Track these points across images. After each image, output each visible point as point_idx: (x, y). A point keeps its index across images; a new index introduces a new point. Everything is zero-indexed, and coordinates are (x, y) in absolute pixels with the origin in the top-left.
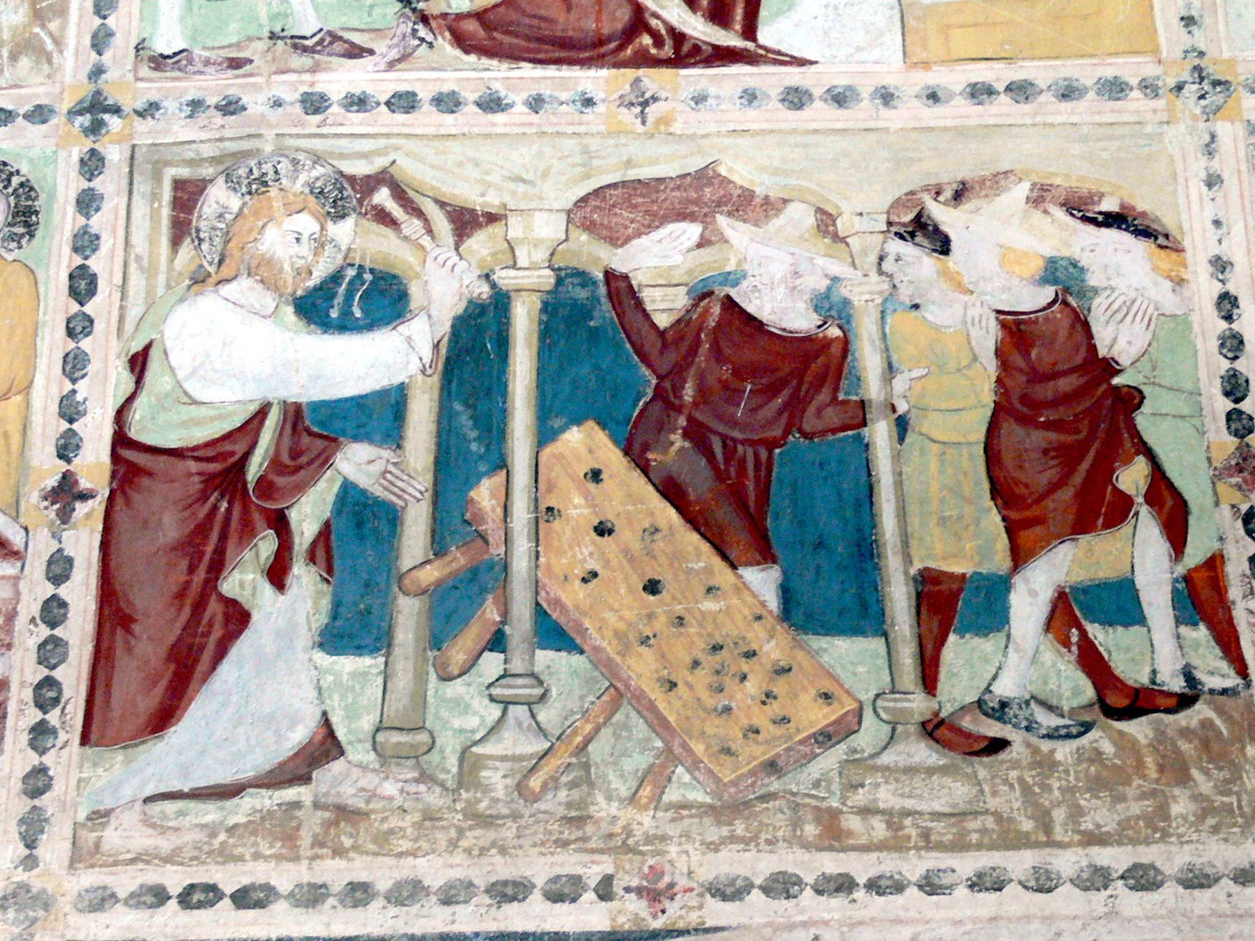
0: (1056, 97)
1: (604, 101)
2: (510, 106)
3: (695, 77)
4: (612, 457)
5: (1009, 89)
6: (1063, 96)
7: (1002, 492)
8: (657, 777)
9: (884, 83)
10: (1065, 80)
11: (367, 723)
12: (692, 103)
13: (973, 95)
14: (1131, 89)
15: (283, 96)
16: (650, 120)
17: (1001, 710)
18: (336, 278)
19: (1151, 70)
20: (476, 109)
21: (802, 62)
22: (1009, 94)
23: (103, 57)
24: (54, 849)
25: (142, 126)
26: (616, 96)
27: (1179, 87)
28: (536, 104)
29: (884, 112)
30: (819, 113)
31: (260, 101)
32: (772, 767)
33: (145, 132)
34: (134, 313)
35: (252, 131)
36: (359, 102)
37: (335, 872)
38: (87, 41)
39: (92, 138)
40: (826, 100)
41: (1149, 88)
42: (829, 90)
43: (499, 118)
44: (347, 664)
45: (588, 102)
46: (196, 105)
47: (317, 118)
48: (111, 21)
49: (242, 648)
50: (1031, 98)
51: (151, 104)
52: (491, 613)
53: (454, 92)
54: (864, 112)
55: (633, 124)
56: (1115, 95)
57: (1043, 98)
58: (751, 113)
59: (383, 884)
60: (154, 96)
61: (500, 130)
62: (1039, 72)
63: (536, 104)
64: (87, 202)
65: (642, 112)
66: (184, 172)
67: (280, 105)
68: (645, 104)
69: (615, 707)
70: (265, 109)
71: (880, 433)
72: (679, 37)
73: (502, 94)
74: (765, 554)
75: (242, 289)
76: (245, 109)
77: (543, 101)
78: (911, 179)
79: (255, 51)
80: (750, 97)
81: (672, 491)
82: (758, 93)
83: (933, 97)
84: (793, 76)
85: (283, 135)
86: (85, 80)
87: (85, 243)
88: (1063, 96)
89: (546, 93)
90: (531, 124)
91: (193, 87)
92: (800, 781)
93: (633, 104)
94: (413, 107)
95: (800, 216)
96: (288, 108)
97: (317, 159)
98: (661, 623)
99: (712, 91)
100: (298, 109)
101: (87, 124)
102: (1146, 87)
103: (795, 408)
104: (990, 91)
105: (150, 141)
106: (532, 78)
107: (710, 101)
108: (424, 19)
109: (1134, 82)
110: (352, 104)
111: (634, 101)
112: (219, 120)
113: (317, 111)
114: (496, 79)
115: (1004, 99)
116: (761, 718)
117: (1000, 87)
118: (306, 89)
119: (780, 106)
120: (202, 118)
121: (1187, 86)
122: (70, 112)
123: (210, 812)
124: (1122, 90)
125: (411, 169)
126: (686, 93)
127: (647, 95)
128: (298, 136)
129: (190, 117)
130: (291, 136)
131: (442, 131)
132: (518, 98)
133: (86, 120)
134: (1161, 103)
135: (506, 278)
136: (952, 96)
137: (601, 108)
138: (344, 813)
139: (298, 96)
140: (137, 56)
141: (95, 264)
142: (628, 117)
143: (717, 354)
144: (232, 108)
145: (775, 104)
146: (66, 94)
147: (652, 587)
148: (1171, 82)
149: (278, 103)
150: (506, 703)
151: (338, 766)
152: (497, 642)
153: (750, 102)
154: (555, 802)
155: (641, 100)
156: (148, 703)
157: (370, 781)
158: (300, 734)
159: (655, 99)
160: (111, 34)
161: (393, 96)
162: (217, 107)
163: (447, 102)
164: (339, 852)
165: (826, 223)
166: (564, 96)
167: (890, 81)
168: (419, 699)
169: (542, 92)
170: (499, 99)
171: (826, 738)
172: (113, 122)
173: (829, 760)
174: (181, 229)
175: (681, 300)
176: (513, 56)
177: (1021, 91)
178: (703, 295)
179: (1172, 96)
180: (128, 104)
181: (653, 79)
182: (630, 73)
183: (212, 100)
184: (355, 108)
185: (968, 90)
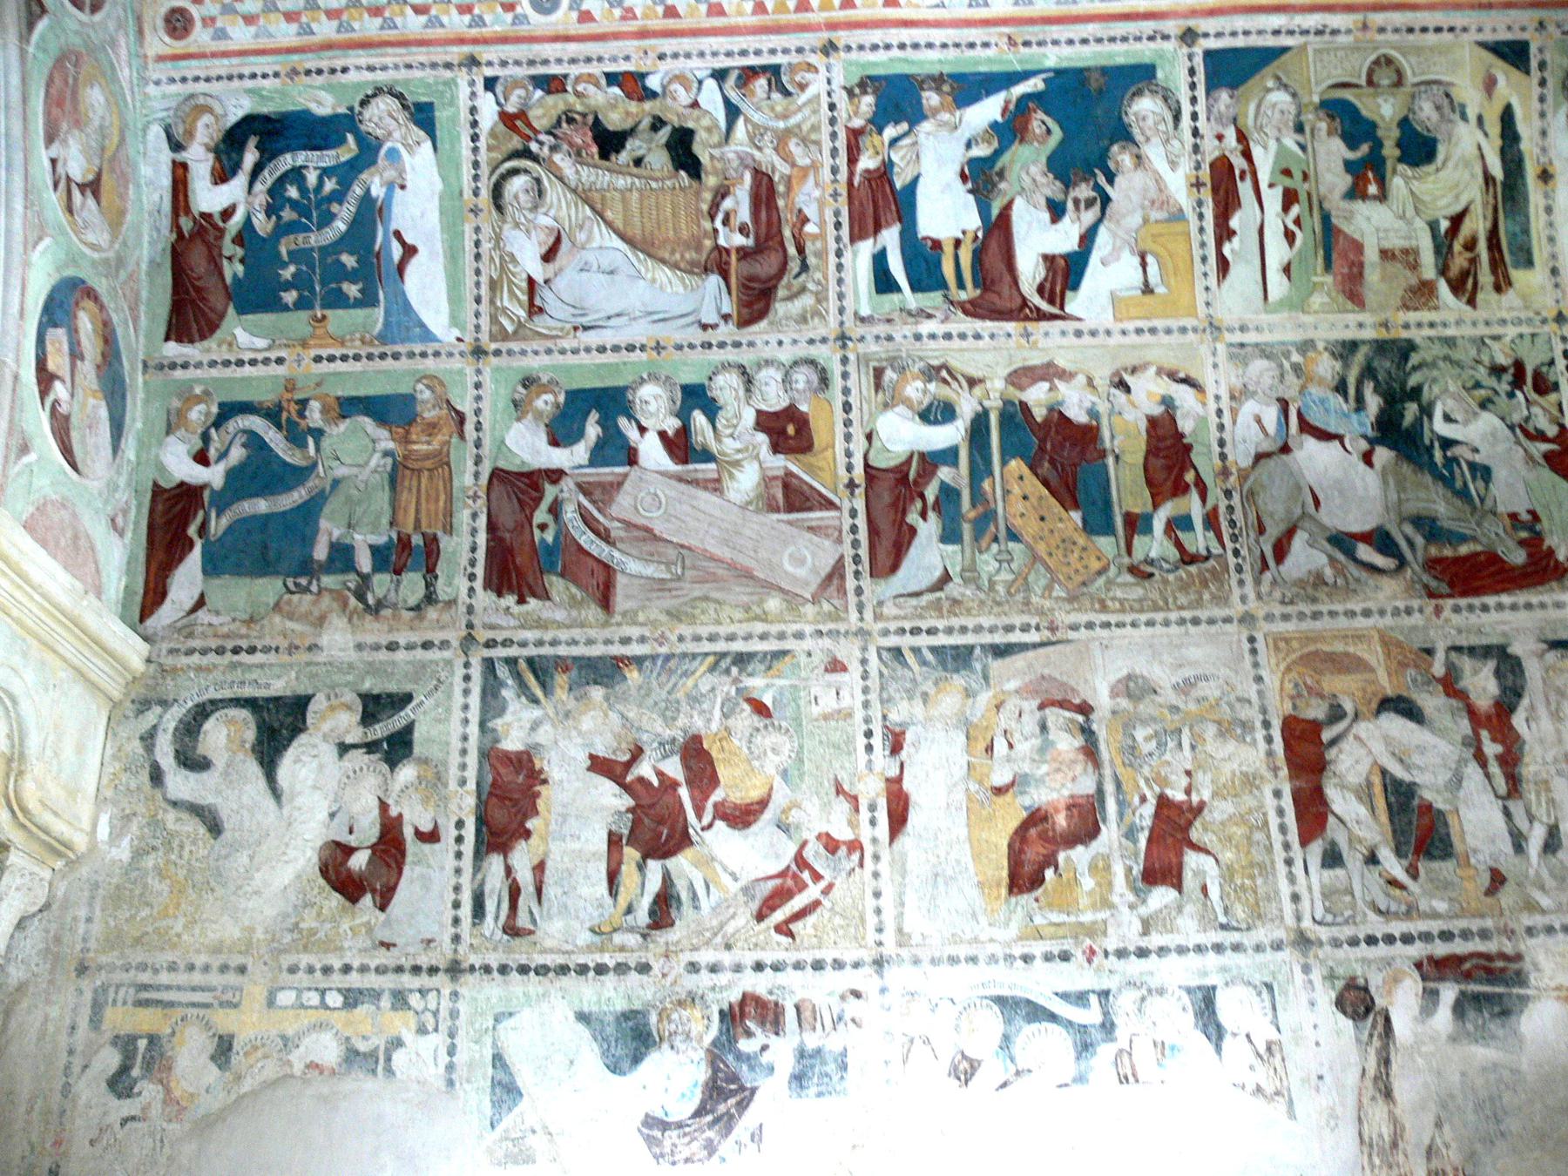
3: (1044, 325)
4: (1026, 471)
7: (1150, 482)
8: (1049, 588)
11: (958, 569)
17: (1151, 562)
18: (931, 405)
19: (1195, 323)
21: (1079, 319)
24: (868, 615)
28: (992, 336)
32: (1084, 584)
33: (861, 348)
34: (866, 418)
36: (933, 336)
37: (956, 622)
41: (1195, 330)
44: (950, 548)
45: (1009, 335)
46: (877, 338)
49: (916, 542)
52: (993, 528)
54: (1101, 338)
59: (971, 626)
62: (1159, 323)
64: (845, 375)
66: (876, 364)
69: (1033, 563)
71: (1110, 461)
72: (1038, 309)
74: (1076, 506)
75: (901, 409)
78: (1118, 364)
79: (896, 315)
81: (1046, 483)
83: (1124, 333)
84: (1076, 325)
87: (846, 391)
92: (1093, 589)
95: (1081, 379)
97: (921, 359)
98: (1046, 532)
103: (1083, 452)
108: (952, 303)
116: (1079, 567)
123: (914, 602)
125: (954, 363)
132: (985, 335)
135: (987, 403)
138: (955, 602)
141: (851, 400)
142: (1023, 341)
143: (1057, 432)
147: (1042, 519)
150: (1000, 562)
151: (951, 585)
152: (996, 539)
154: (1019, 597)
156: (889, 563)
157: (962, 590)
158: (938, 573)
163: (963, 336)
164: (956, 615)
165: (1090, 382)
168: (973, 561)
171: (1099, 573)
172: (850, 344)
173: (1101, 581)
174: (878, 386)
175: (1044, 412)
176: (982, 317)
177: (1153, 331)
178: (1051, 409)
181: (1030, 326)
182: (1022, 324)
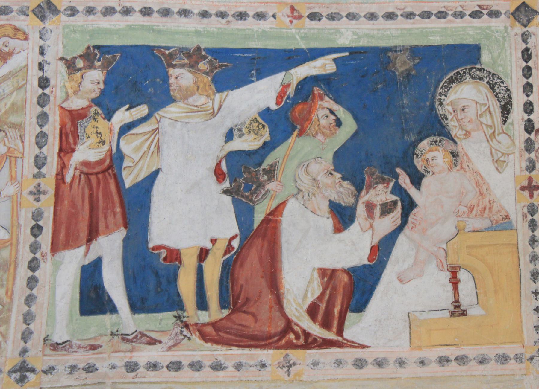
0: (477, 363)
1: (270, 365)
2: (226, 368)
3: (314, 353)
5: (456, 359)
6: (480, 362)
9: (401, 357)
10: (481, 355)
12: (312, 366)
13: (440, 362)
14: (511, 359)
15: (116, 363)
16: (292, 374)
19: (519, 350)
20: (210, 369)
21: (363, 347)
22: (456, 361)
23: (27, 344)
25: (46, 378)
26: (276, 363)
27: (532, 358)
28: (238, 367)
29: (401, 370)
30: (370, 371)
31: (105, 366)
35: (100, 380)
36: (153, 366)
38: (19, 336)
39: (20, 384)
40: (373, 364)
41: (518, 359)
42: (375, 360)
43: (221, 373)
45: (263, 366)
46: (73, 368)
47: (133, 374)
48: (32, 326)
50: (466, 363)
51: (50, 368)
53: (199, 361)
54: (391, 370)
55: (284, 376)
56: (503, 362)
57: (471, 363)
58: (339, 371)
60: (52, 364)
61: (221, 379)
62: (470, 351)
63: (238, 367)
65: (288, 370)
67: (114, 368)
68: (290, 366)
70: (108, 370)
73: (222, 362)
76: (97, 370)
77: (242, 365)
79: (103, 341)
80: (339, 363)
82: (342, 361)
83: (422, 363)
84: (359, 353)
85: (116, 383)
86: (18, 356)
88: (480, 362)
89: (243, 361)
90: (235, 377)
91: (72, 359)
93: (284, 367)
94: (179, 369)
96: (118, 370)
99: (321, 360)
100: (123, 370)
101: (18, 377)
102: (517, 358)
104: (448, 360)
105: (49, 386)
106: (237, 354)
107: (320, 365)
108: (187, 326)
109: (512, 356)
110: (150, 367)
111: (285, 365)
112: (84, 375)
113: (132, 371)
114: (220, 355)
115: (454, 363)
117: (452, 358)
118: (128, 360)
119: (352, 367)
120: (76, 374)
121: (535, 358)
122: (9, 372)
124: (506, 360)
126: (309, 361)
127: (291, 362)
128: (123, 383)
129: (70, 373)
130: (119, 383)
131: (193, 380)
132: (230, 364)
133: (17, 375)
134: (523, 366)
136: (431, 362)
137: (269, 369)
139: (123, 363)
140: (44, 344)
142: (282, 372)
144: (91, 369)
145: (350, 366)
146: (7, 363)
148: (528, 356)
149: (113, 367)
153: (339, 365)
155: (288, 364)
159: (294, 364)
160: (31, 333)
161: (170, 363)
162: (83, 369)
163: (196, 366)
166: (252, 363)
167: (402, 355)
169: (241, 361)
170: (221, 364)
172: (31, 376)
176: (228, 343)
177: (462, 360)
179: (528, 362)
180: (39, 367)
181: (294, 355)
182: (284, 352)
183: (81, 366)
184: (151, 369)
185: (438, 359)
